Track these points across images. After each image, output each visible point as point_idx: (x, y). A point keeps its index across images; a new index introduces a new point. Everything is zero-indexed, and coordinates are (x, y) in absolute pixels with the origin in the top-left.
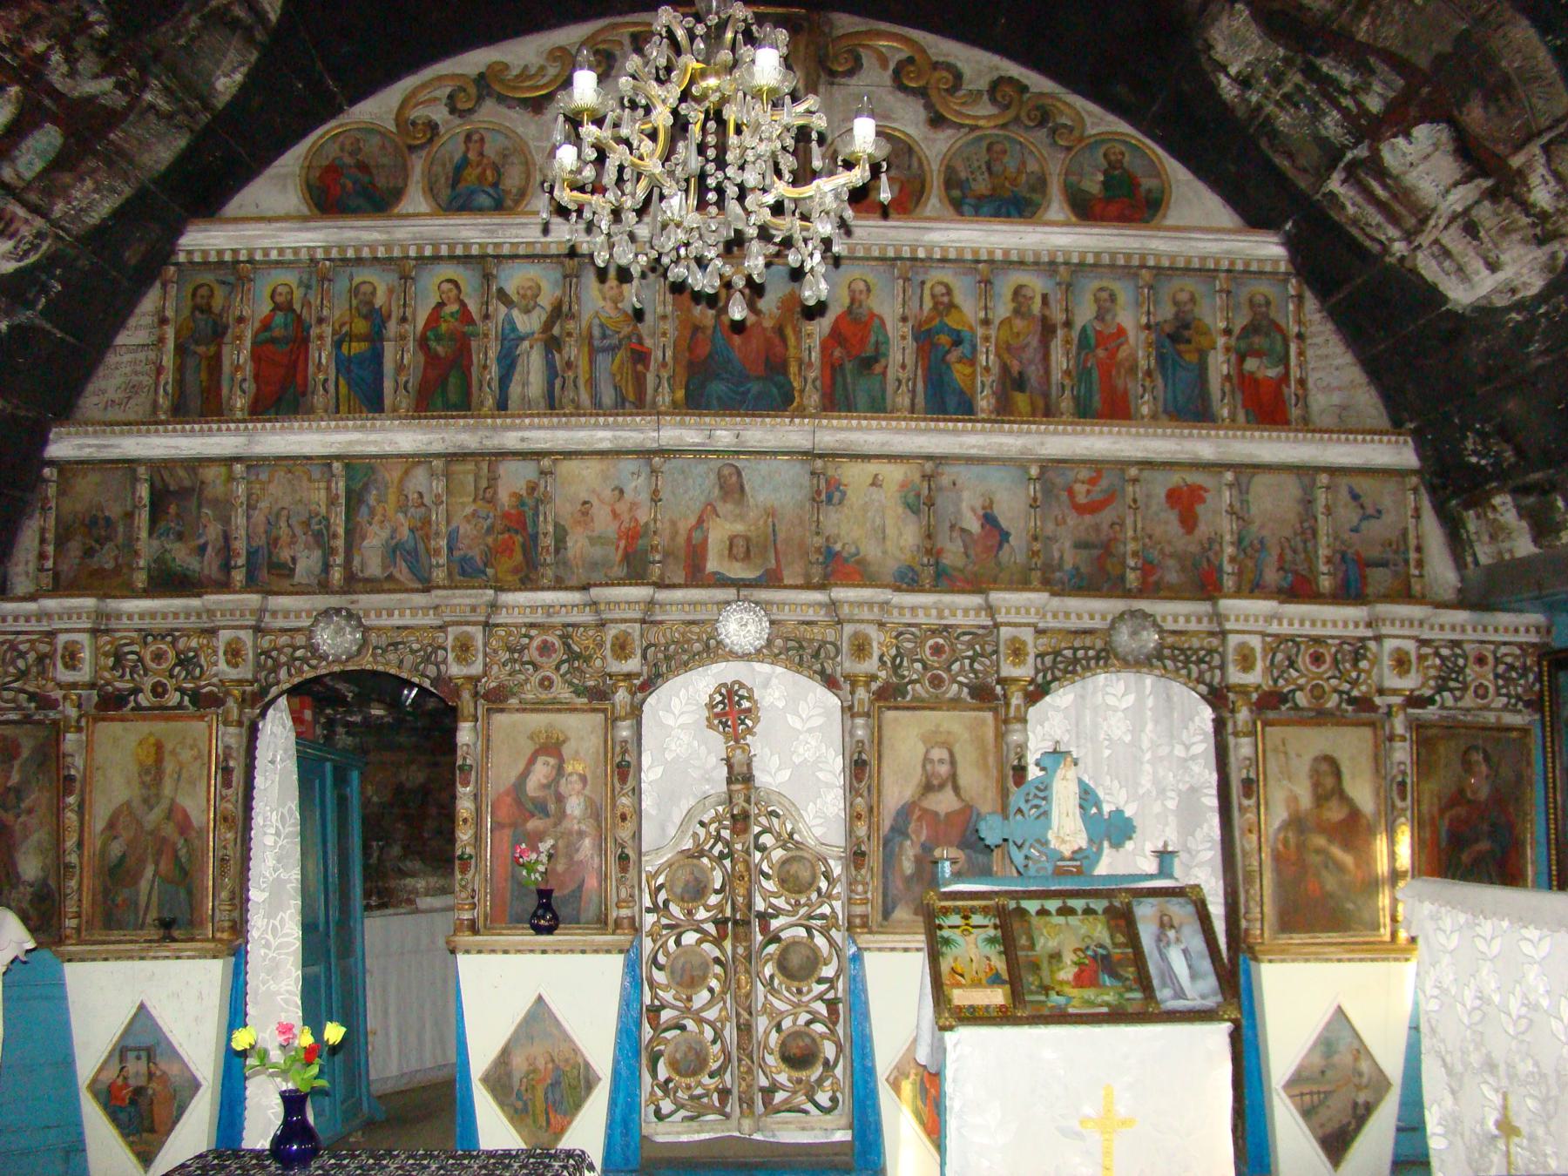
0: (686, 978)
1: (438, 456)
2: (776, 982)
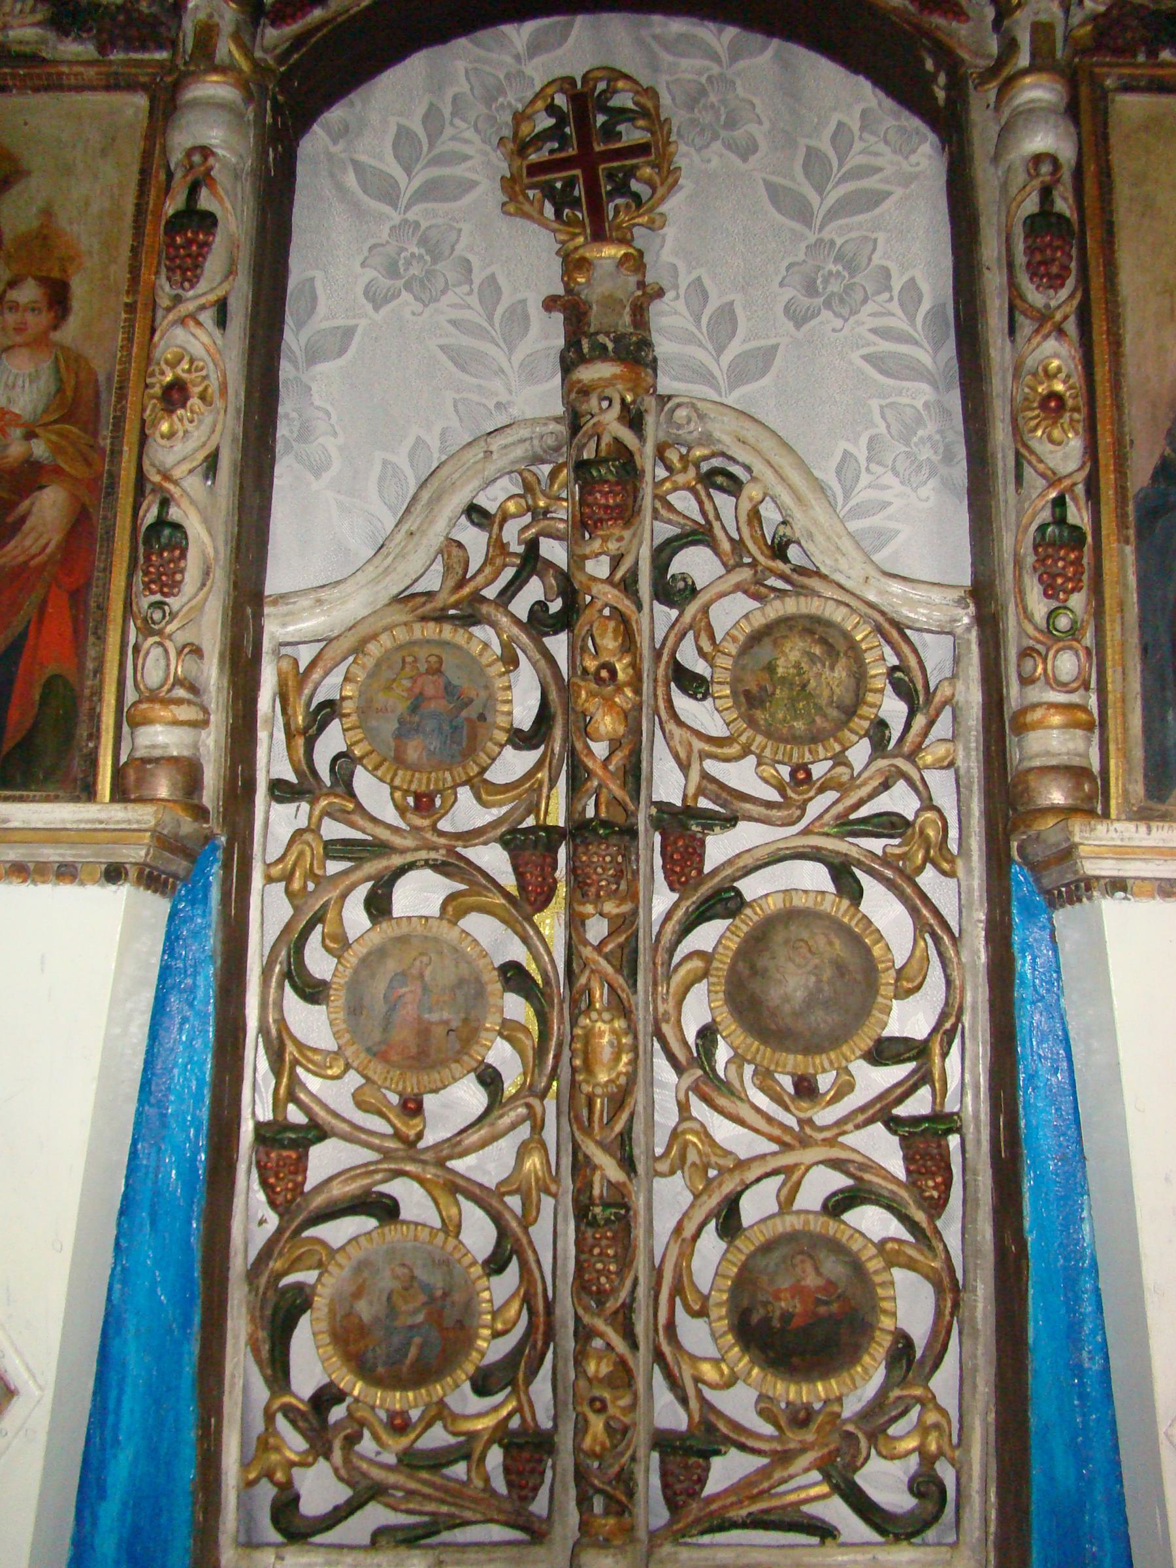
0: (403, 1035)
2: (722, 1053)
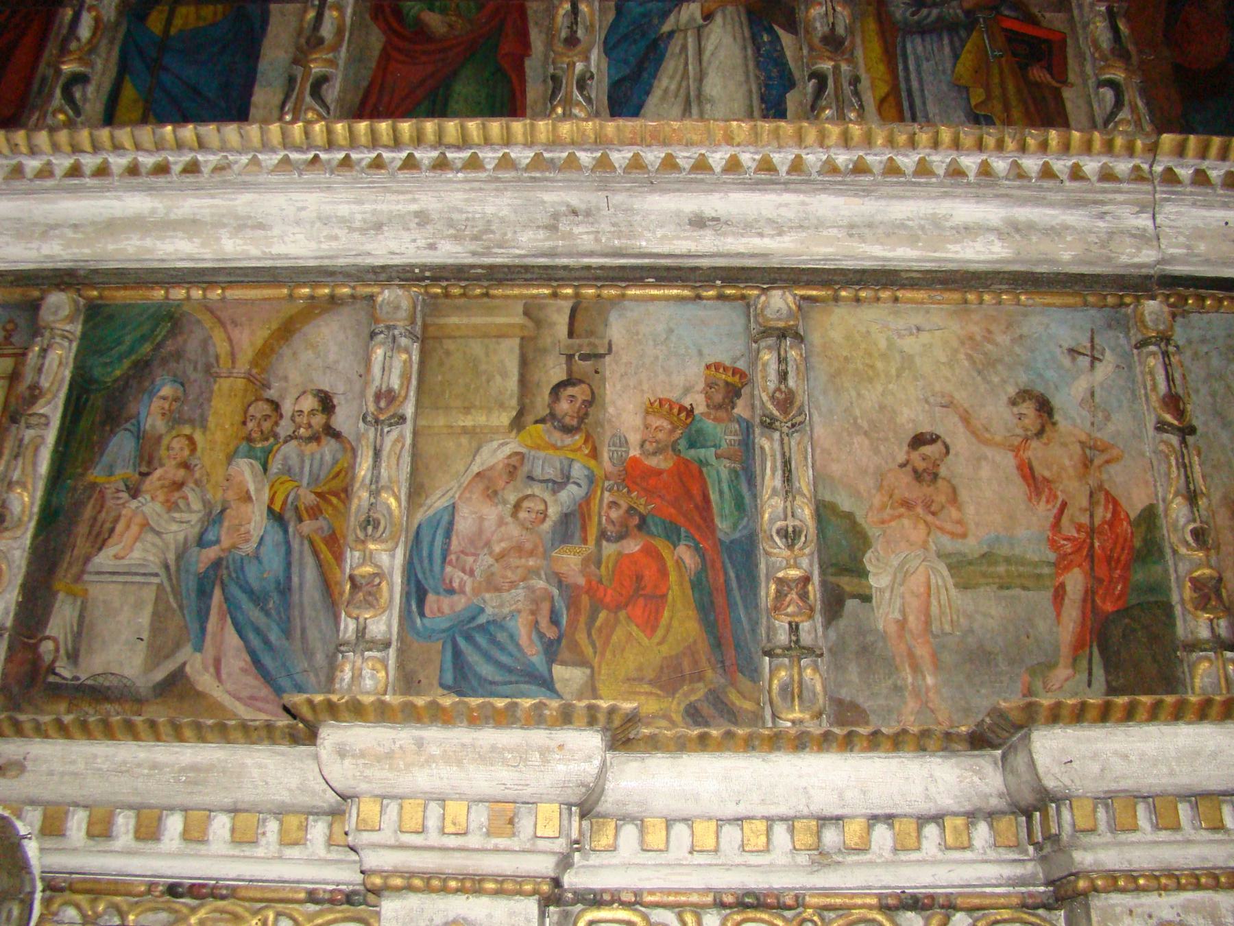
1: (406, 275)
